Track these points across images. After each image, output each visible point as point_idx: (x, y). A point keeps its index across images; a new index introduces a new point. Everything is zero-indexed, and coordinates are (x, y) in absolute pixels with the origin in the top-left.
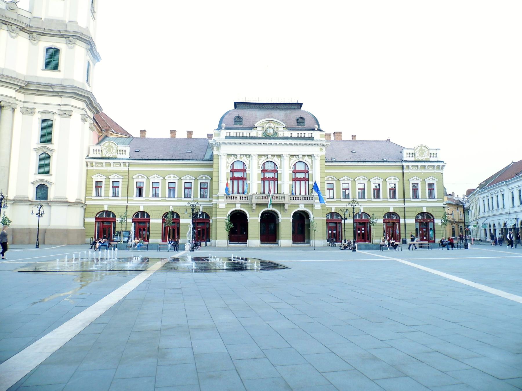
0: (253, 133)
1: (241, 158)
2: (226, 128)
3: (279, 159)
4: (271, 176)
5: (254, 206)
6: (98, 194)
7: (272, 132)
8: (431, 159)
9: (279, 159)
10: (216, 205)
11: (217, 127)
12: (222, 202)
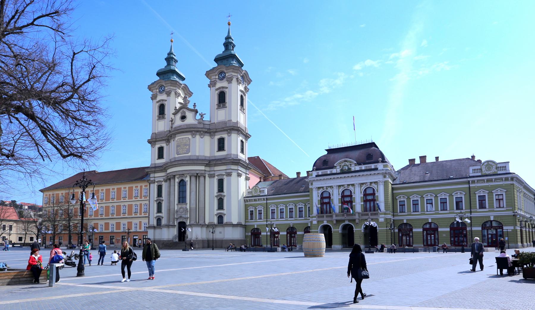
0: (334, 171)
1: (327, 189)
2: (317, 170)
4: (347, 199)
5: (335, 222)
6: (252, 219)
7: (347, 168)
8: (499, 172)
10: (311, 222)
12: (314, 220)
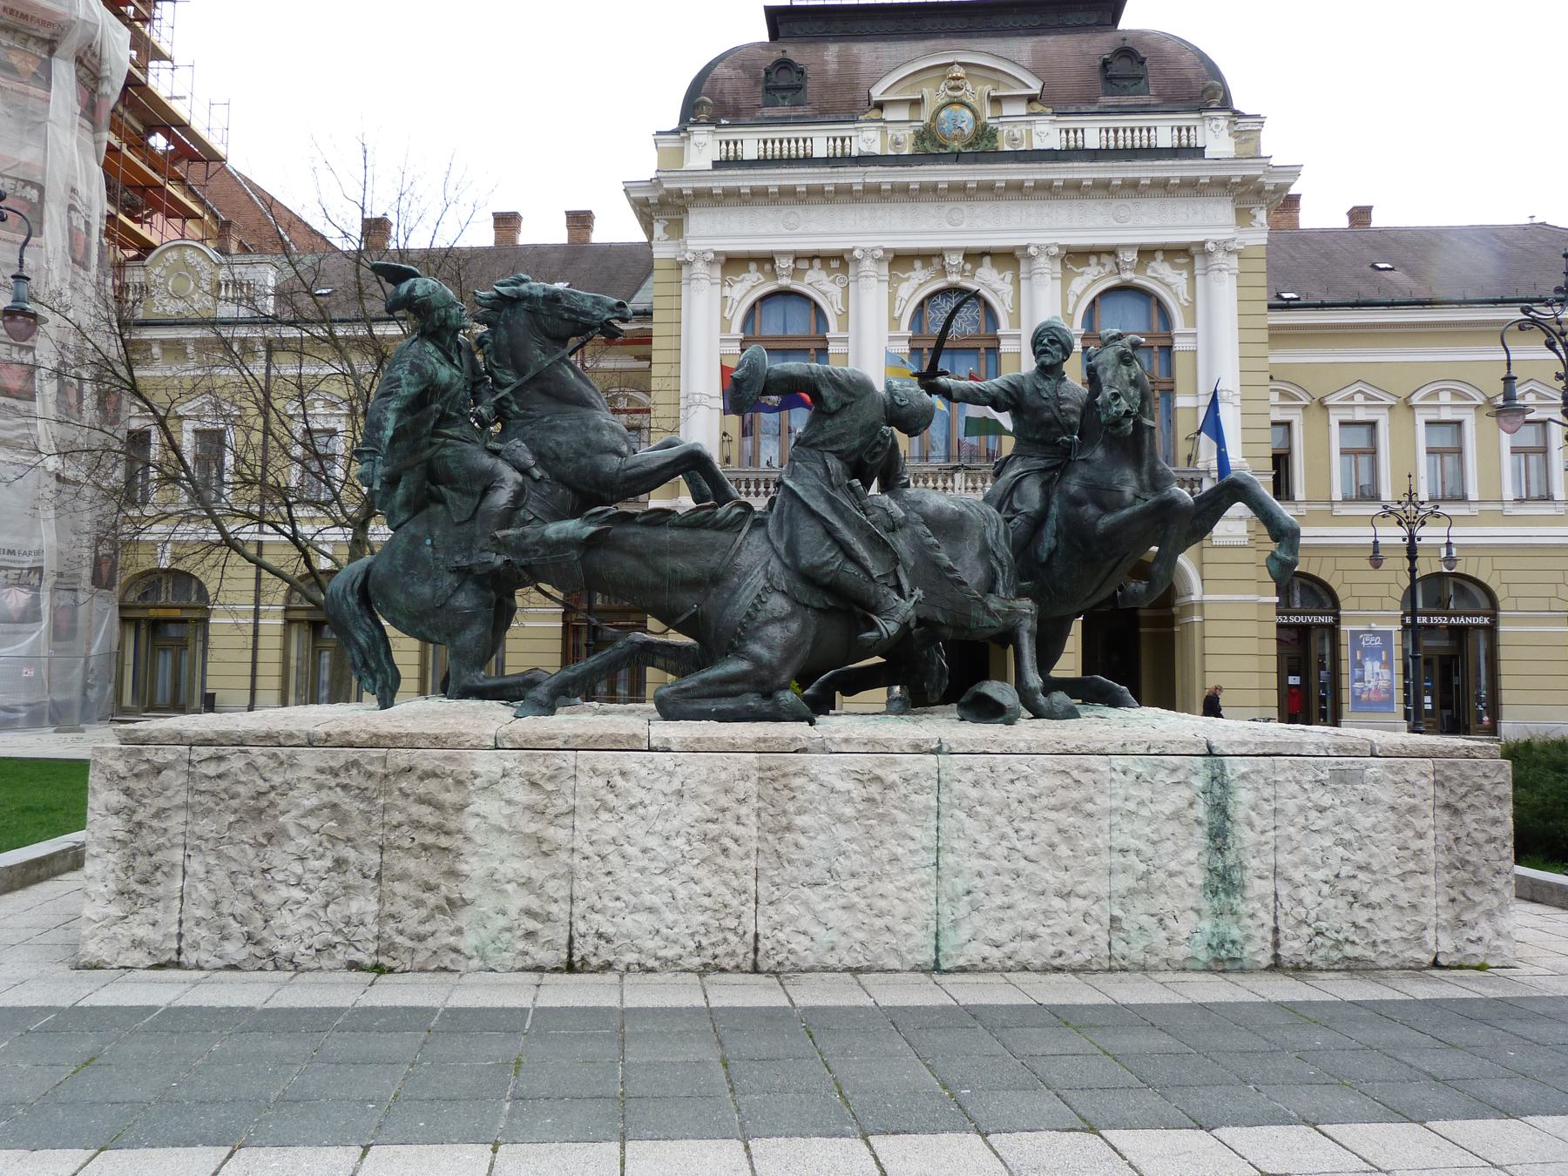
0: (866, 139)
3: (1009, 276)
9: (1009, 276)
11: (673, 122)
